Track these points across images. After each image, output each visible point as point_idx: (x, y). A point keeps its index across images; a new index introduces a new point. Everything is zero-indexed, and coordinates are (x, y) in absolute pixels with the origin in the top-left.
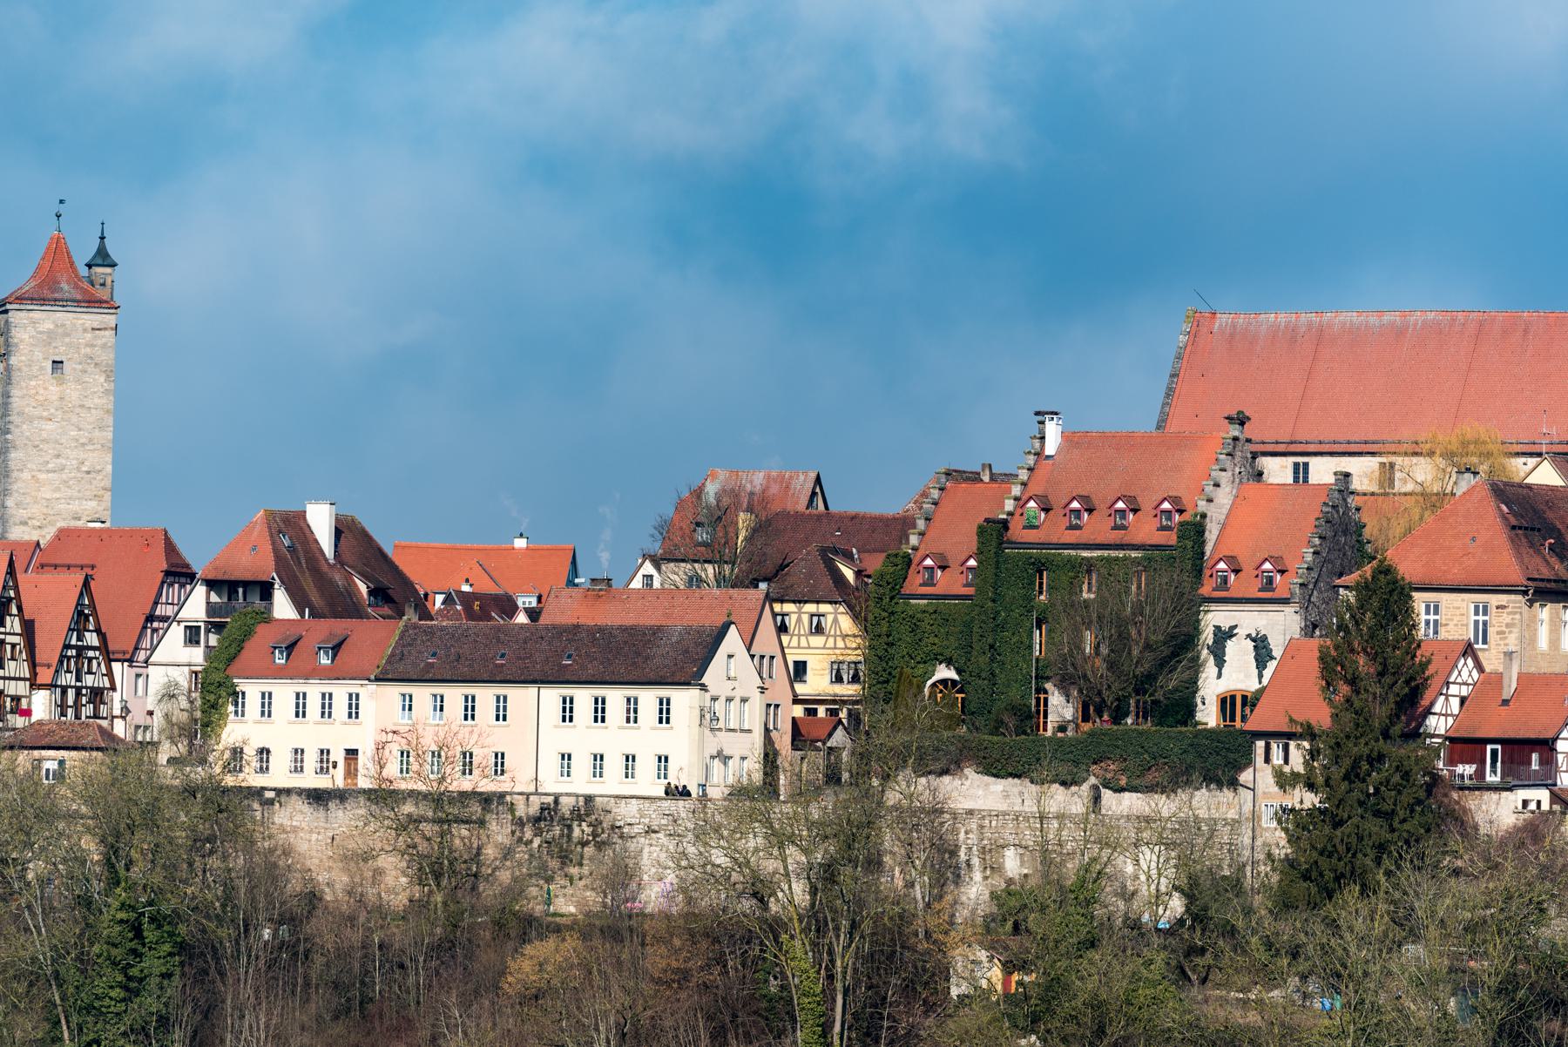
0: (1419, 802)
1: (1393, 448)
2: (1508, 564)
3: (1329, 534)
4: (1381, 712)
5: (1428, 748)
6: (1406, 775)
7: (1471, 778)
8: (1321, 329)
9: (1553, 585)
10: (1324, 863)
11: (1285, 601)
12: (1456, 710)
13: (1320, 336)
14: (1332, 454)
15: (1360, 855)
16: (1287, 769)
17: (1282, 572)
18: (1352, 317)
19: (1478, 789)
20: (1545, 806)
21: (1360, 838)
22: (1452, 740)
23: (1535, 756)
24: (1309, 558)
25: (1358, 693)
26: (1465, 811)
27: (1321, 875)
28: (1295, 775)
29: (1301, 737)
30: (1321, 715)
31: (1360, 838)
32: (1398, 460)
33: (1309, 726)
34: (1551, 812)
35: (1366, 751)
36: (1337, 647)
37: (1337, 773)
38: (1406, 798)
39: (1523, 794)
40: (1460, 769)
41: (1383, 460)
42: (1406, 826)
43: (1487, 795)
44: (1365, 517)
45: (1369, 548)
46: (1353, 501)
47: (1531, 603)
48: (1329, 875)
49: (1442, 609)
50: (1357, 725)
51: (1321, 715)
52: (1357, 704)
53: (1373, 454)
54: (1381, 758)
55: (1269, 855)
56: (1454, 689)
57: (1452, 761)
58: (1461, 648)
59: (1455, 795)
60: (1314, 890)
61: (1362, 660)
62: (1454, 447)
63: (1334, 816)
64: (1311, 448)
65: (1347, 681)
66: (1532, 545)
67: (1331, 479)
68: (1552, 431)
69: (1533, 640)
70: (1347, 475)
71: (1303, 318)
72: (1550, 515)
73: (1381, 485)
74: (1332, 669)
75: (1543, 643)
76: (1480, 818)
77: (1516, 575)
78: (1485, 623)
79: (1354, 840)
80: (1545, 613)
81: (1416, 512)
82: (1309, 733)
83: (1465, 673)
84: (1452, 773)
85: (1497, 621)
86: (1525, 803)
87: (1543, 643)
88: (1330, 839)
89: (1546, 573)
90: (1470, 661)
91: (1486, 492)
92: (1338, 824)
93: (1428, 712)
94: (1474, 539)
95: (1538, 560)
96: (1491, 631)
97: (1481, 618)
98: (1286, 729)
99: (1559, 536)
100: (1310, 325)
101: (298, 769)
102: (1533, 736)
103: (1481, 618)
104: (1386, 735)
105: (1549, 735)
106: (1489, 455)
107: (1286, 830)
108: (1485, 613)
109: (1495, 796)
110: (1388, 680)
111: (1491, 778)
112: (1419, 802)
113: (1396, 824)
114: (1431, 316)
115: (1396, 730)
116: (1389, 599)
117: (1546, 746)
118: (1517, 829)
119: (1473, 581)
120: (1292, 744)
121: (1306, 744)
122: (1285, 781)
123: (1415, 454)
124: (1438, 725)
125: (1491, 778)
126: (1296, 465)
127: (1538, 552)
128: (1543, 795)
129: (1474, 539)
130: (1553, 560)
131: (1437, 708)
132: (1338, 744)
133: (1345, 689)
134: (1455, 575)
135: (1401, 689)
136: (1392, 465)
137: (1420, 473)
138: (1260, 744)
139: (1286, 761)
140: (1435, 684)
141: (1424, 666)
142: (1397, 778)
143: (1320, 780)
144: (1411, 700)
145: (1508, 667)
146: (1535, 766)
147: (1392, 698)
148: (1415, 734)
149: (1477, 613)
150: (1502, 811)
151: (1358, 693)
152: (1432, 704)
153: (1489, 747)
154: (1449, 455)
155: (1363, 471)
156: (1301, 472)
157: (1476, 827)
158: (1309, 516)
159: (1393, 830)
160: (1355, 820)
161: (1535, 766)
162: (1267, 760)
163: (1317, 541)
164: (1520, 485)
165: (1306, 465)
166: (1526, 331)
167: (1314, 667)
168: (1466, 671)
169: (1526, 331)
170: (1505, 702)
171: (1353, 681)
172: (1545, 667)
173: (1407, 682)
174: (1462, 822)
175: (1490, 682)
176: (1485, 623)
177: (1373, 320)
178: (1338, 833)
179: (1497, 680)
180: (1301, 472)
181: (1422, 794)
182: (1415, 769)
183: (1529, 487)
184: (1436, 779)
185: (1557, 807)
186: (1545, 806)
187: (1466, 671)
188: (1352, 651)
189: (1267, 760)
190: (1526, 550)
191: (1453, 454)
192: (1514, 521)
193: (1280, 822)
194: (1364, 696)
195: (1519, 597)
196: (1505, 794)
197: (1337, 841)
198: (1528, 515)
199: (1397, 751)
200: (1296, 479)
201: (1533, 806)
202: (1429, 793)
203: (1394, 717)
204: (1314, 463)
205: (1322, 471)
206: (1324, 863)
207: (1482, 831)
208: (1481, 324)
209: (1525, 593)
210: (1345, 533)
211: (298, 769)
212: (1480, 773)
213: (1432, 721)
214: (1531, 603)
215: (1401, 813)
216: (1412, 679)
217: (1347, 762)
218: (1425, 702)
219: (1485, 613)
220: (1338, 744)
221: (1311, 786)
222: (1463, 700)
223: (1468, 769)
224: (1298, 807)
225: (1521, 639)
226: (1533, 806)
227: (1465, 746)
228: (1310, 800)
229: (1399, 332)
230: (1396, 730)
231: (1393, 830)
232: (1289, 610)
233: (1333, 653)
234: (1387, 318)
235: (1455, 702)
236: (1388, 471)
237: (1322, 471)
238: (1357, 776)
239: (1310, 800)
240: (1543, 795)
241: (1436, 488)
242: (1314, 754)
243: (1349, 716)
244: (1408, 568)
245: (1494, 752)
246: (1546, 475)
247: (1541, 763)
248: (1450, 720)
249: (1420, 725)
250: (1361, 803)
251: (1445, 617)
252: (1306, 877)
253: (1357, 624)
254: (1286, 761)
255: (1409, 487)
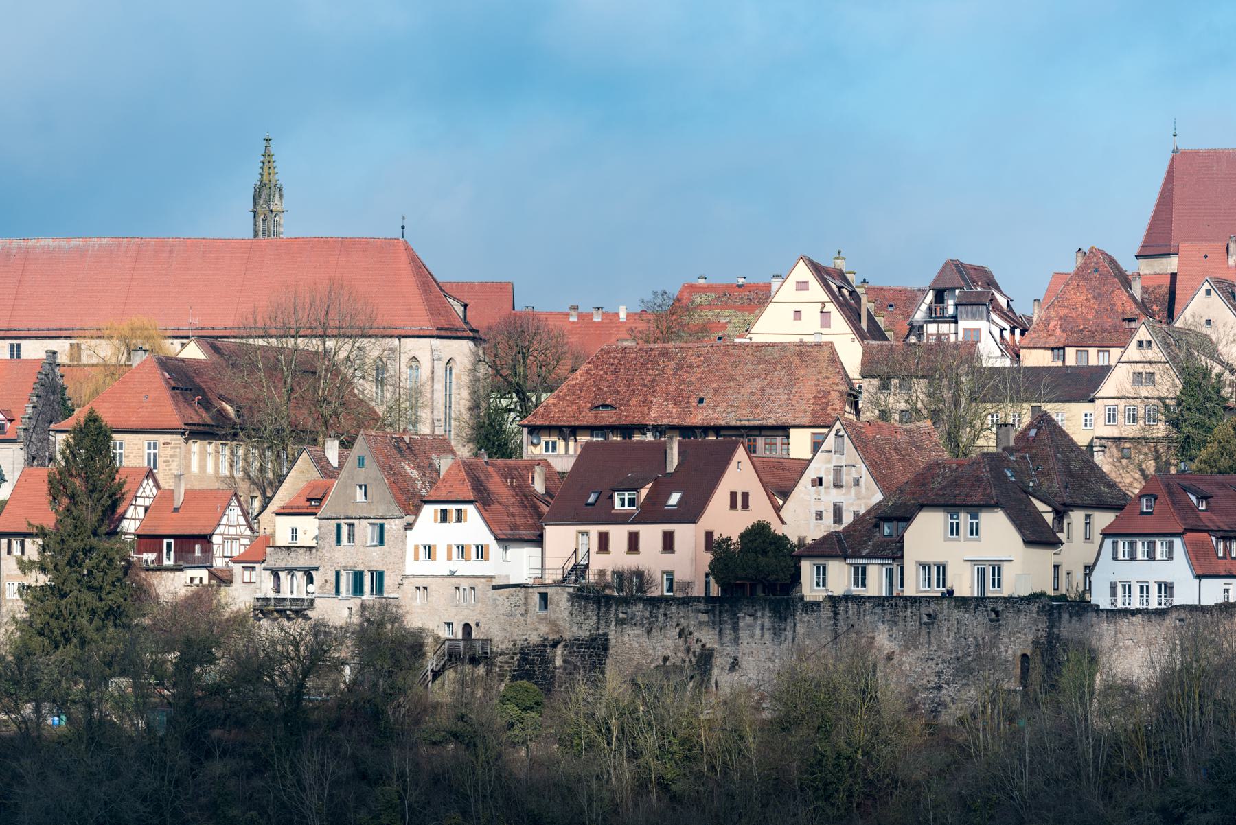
0: (119, 580)
1: (80, 333)
2: (171, 414)
3: (43, 394)
4: (92, 518)
5: (124, 542)
6: (111, 561)
7: (153, 562)
8: (27, 252)
9: (201, 428)
10: (53, 623)
11: (13, 441)
12: (142, 516)
13: (27, 256)
14: (36, 338)
15: (78, 618)
16: (25, 558)
17: (11, 421)
18: (48, 242)
19: (159, 570)
20: (205, 581)
21: (79, 606)
22: (139, 536)
23: (197, 547)
24: (30, 411)
25: (75, 504)
26: (150, 585)
27: (52, 632)
28: (32, 563)
29: (37, 536)
30: (48, 519)
31: (79, 606)
32: (84, 343)
33: (42, 528)
34: (210, 585)
35: (82, 545)
36: (60, 473)
37: (62, 560)
38: (110, 578)
39: (190, 573)
40: (145, 556)
41: (74, 341)
42: (111, 597)
43: (165, 574)
44: (65, 382)
45: (69, 403)
46: (58, 371)
47: (187, 440)
48: (57, 632)
49: (125, 445)
50: (76, 527)
51: (48, 519)
52: (75, 513)
53: (66, 337)
54: (92, 548)
55: (14, 618)
56: (140, 501)
57: (140, 552)
58: (145, 473)
59: (143, 575)
60: (46, 642)
61: (78, 482)
62: (127, 332)
63: (60, 590)
64: (22, 334)
65: (67, 496)
66: (186, 400)
67: (43, 356)
68: (193, 320)
69: (189, 466)
70: (55, 353)
71: (15, 243)
72: (197, 379)
73: (72, 359)
74: (57, 487)
75: (195, 468)
76: (161, 591)
77: (176, 421)
78: (155, 455)
79: (74, 607)
80: (196, 447)
81: (101, 378)
82: (42, 533)
83: (148, 490)
84: (140, 560)
85: (163, 454)
86: (192, 579)
87: (195, 468)
88: (58, 607)
89: (197, 420)
90: (151, 481)
91: (154, 364)
92: (63, 596)
93: (123, 517)
94: (146, 397)
95: (190, 411)
96: (158, 460)
97: (152, 451)
98: (25, 530)
99: (204, 393)
100: (19, 248)
101: (623, 505)
102: (196, 532)
103: (152, 451)
104: (95, 534)
105: (207, 532)
106: (149, 338)
107: (26, 601)
108: (155, 448)
109: (171, 575)
110: (96, 495)
111: (166, 562)
112: (119, 580)
113: (103, 596)
114: (104, 241)
115: (103, 530)
116: (95, 439)
117: (206, 539)
118: (187, 599)
119: (147, 426)
120: (28, 541)
121: (40, 541)
122: (24, 567)
123: (99, 337)
124: (129, 526)
125: (166, 562)
126: (12, 346)
127: (190, 405)
128: (204, 574)
129: (146, 397)
130: (201, 411)
131: (128, 515)
132: (63, 541)
133: (65, 501)
134: (134, 422)
135: (106, 501)
136: (79, 345)
137: (101, 351)
138: (4, 541)
139: (23, 553)
140: (128, 497)
141: (121, 485)
142: (104, 563)
143: (51, 566)
144: (112, 509)
145: (178, 486)
146: (198, 554)
147: (99, 508)
148: (113, 533)
149: (149, 448)
150: (174, 585)
151: (75, 504)
152: (125, 512)
153: (165, 541)
154: (123, 338)
155: (62, 347)
156: (15, 351)
157: (157, 597)
158: (30, 381)
159: (101, 600)
160: (75, 593)
161: (198, 554)
162: (9, 552)
163: (35, 399)
164: (177, 359)
165: (19, 346)
166: (171, 252)
167: (44, 488)
168: (148, 488)
169: (171, 252)
170: (176, 510)
171: (72, 497)
172: (197, 486)
173: (110, 497)
174: (143, 593)
175: (165, 496)
176: (155, 455)
177: (64, 244)
178: (64, 602)
179: (170, 494)
180: (15, 351)
181: (121, 575)
182: (117, 557)
183: (182, 360)
184: (130, 564)
185: (214, 582)
186: (205, 581)
187: (148, 488)
188: (71, 475)
189: (9, 552)
190: (182, 404)
191: (126, 338)
192: (173, 384)
193: (21, 594)
194: (80, 507)
195: (179, 437)
196: (178, 573)
197: (63, 608)
198: (183, 380)
199: (105, 545)
200: (12, 356)
201: (197, 581)
202: (125, 574)
203: (101, 521)
204: (23, 343)
205: (33, 350)
206: (53, 623)
207: (161, 600)
208: (139, 247)
209: (183, 433)
210: (53, 393)
211: (623, 505)
212: (160, 559)
213: (125, 523)
214: (187, 440)
215: (108, 588)
216: (114, 494)
217: (69, 553)
218: (120, 510)
219: (155, 448)
220: (63, 541)
221: (43, 570)
222: (146, 509)
223: (151, 557)
224: (33, 584)
225: (180, 465)
226: (197, 581)
227: (149, 540)
228: (43, 579)
229: (82, 253)
230: (103, 530)
231: (101, 600)
232: (16, 447)
233: (58, 477)
234: (74, 242)
235: (141, 511)
236: (76, 351)
237: (33, 350)
238: (76, 562)
239: (43, 579)
240: (204, 574)
241: (113, 361)
242: (44, 548)
243: (69, 521)
244: (107, 417)
245: (169, 545)
246: (193, 352)
247: (202, 551)
248: (138, 523)
249: (117, 526)
250: (79, 581)
251: (132, 451)
252: (41, 633)
253: (74, 457)
254: (23, 553)
255: (94, 361)
